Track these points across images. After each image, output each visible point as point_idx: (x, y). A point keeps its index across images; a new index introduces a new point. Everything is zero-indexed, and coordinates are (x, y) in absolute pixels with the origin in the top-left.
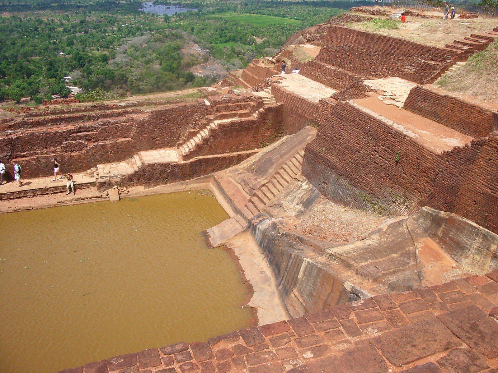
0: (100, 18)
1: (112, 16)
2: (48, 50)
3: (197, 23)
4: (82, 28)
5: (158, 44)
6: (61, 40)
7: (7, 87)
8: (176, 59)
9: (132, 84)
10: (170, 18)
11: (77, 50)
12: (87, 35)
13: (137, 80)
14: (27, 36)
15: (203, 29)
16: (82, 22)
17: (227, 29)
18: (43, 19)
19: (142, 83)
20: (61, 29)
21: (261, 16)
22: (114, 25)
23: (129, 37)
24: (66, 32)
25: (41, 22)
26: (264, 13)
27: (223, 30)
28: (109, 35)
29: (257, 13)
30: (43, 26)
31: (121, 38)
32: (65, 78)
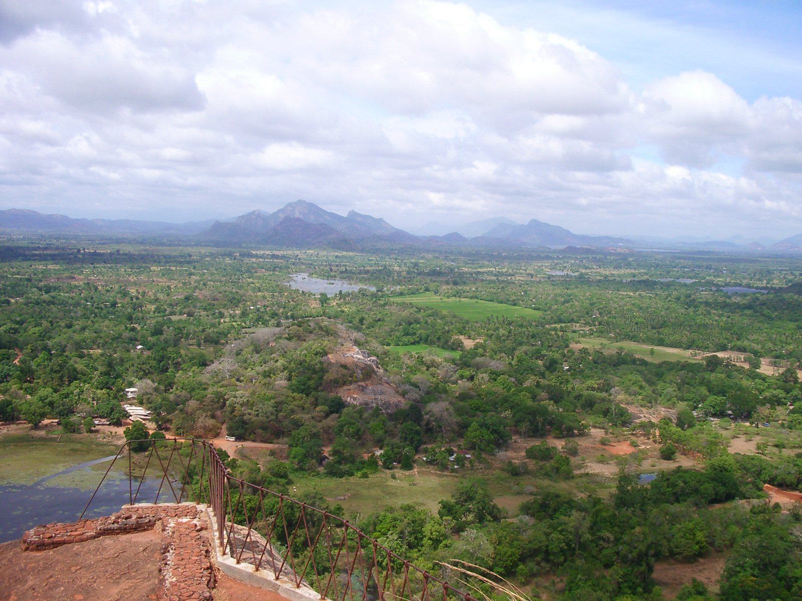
0: (216, 293)
3: (370, 310)
4: (185, 307)
5: (291, 344)
7: (29, 397)
8: (315, 372)
9: (233, 411)
10: (328, 299)
12: (189, 319)
13: (242, 405)
14: (96, 316)
15: (379, 320)
16: (187, 298)
19: (249, 411)
20: (153, 307)
22: (237, 306)
25: (125, 294)
26: (482, 298)
27: (410, 324)
28: (225, 322)
29: (472, 298)
30: (128, 299)
32: (127, 390)
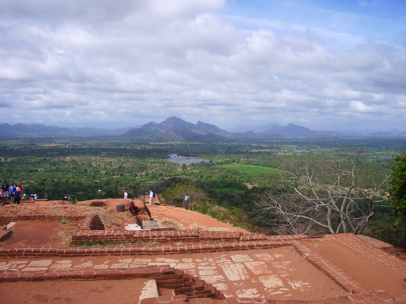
0: (133, 165)
1: (143, 164)
2: (90, 187)
3: (206, 171)
4: (119, 172)
6: (101, 180)
10: (186, 167)
11: (112, 188)
12: (121, 178)
14: (78, 177)
15: (210, 177)
16: (120, 168)
17: (227, 177)
18: (93, 164)
20: (104, 172)
21: (257, 167)
22: (143, 171)
23: (152, 180)
24: (107, 174)
25: (91, 166)
26: (260, 165)
27: (224, 178)
28: (138, 179)
29: (255, 165)
30: (92, 169)
31: (146, 181)
